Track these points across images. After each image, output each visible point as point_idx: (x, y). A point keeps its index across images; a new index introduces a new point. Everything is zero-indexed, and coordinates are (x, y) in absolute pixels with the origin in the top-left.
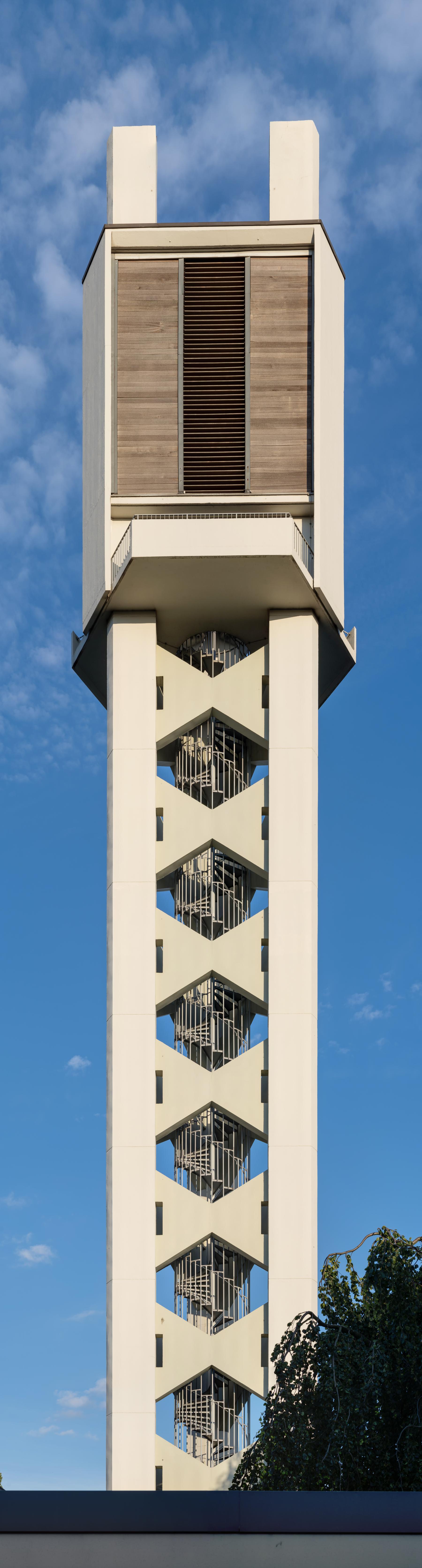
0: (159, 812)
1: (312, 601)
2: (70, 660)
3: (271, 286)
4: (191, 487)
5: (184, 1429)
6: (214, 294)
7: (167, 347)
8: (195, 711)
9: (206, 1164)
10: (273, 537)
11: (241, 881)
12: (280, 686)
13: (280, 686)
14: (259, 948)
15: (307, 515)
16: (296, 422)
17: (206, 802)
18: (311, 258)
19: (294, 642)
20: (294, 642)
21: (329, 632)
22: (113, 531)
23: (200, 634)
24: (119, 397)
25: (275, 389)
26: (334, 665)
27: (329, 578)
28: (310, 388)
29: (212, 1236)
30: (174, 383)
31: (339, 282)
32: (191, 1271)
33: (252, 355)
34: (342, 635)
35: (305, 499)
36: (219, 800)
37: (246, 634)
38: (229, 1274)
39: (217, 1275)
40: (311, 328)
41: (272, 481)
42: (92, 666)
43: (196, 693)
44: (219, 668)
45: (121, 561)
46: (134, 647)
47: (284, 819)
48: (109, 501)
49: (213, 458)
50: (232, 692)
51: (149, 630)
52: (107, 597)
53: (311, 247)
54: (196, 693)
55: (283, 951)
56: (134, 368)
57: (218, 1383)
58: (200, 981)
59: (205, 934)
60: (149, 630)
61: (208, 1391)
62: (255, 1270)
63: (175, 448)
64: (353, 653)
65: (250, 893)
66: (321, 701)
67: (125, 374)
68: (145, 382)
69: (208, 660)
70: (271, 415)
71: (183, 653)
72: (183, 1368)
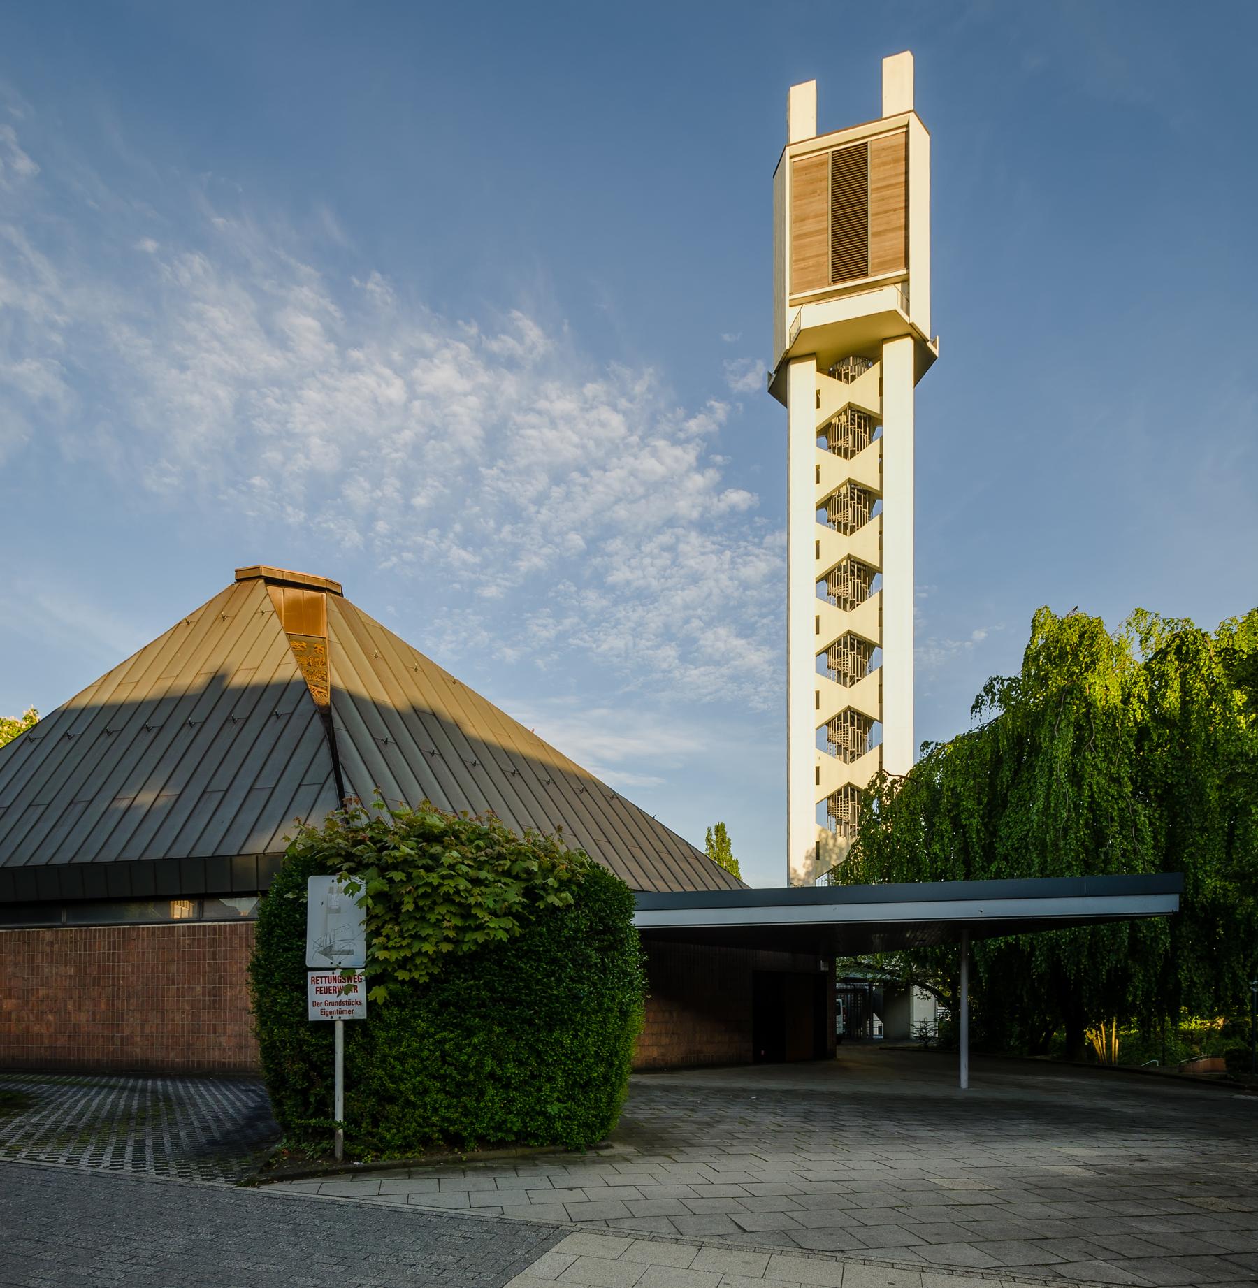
0: (818, 392)
1: (910, 330)
2: (766, 386)
3: (884, 154)
4: (835, 280)
5: (833, 820)
6: (849, 170)
7: (823, 204)
8: (841, 404)
9: (845, 739)
10: (885, 300)
11: (865, 499)
12: (893, 383)
13: (893, 383)
14: (877, 536)
15: (905, 281)
16: (899, 228)
17: (846, 457)
18: (907, 132)
19: (899, 355)
20: (899, 355)
21: (921, 345)
22: (790, 314)
23: (843, 359)
24: (795, 238)
25: (886, 212)
26: (924, 359)
27: (921, 317)
28: (907, 207)
29: (849, 557)
30: (827, 223)
31: (925, 138)
32: (837, 728)
33: (871, 196)
34: (929, 344)
35: (904, 272)
36: (853, 530)
37: (870, 354)
38: (859, 728)
39: (853, 729)
40: (907, 172)
41: (885, 265)
42: (779, 388)
43: (839, 395)
44: (853, 378)
45: (795, 331)
46: (803, 376)
47: (894, 462)
48: (788, 298)
49: (849, 259)
50: (861, 391)
51: (812, 364)
52: (787, 352)
53: (907, 126)
54: (839, 395)
55: (894, 538)
56: (802, 220)
57: (853, 790)
58: (841, 486)
59: (845, 533)
60: (812, 364)
61: (846, 796)
62: (875, 724)
63: (828, 260)
64: (936, 352)
65: (872, 503)
66: (916, 382)
67: (801, 218)
68: (810, 226)
69: (846, 375)
70: (883, 228)
71: (831, 374)
72: (832, 633)
